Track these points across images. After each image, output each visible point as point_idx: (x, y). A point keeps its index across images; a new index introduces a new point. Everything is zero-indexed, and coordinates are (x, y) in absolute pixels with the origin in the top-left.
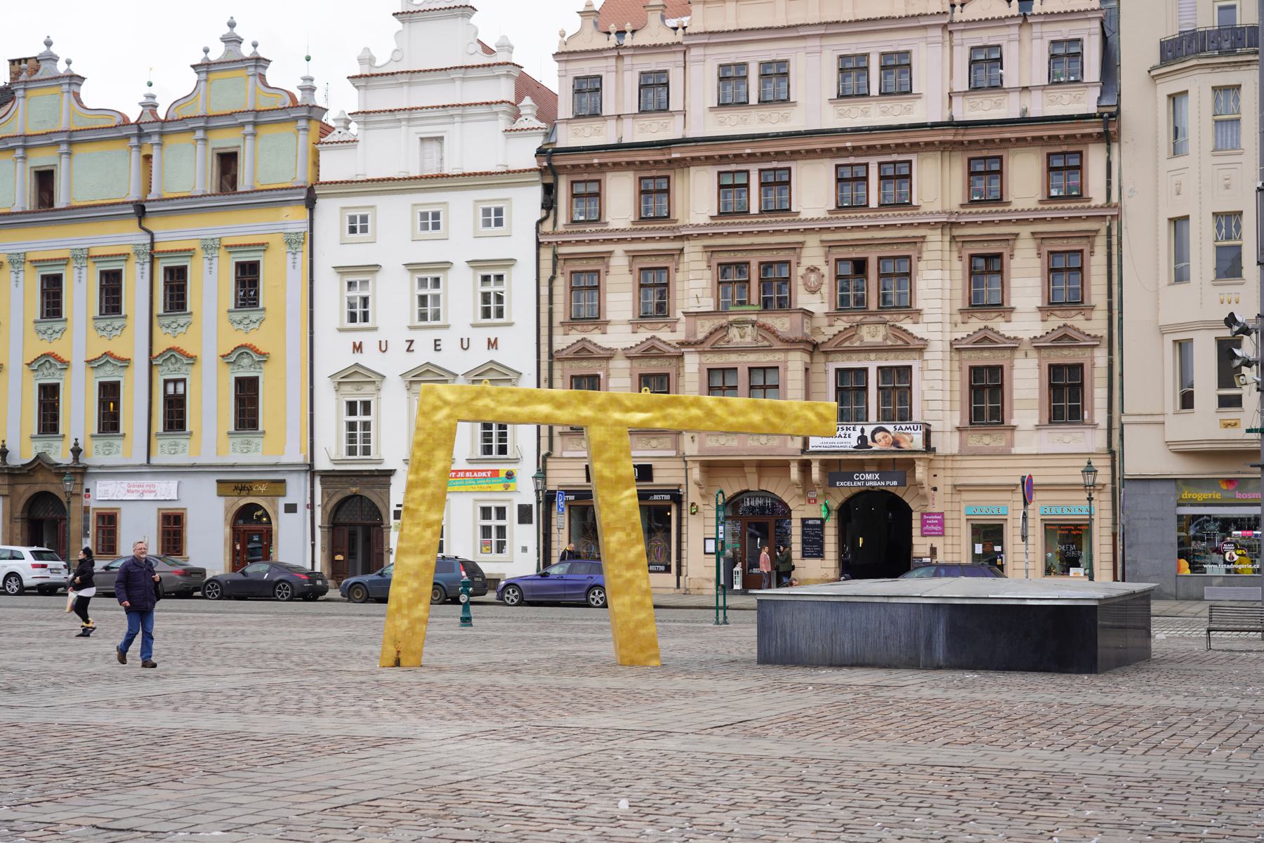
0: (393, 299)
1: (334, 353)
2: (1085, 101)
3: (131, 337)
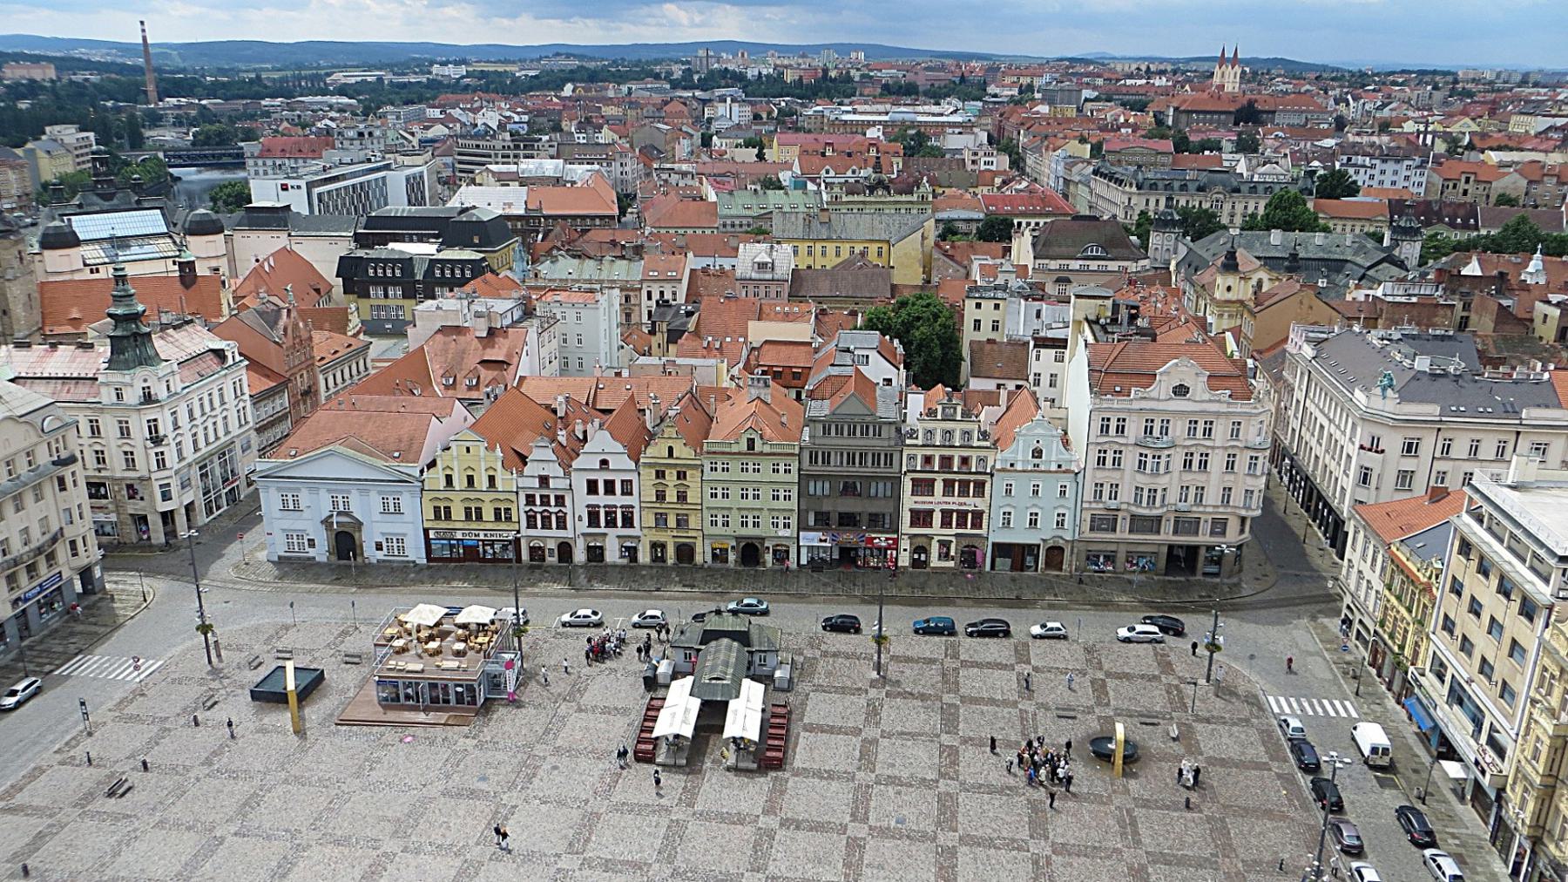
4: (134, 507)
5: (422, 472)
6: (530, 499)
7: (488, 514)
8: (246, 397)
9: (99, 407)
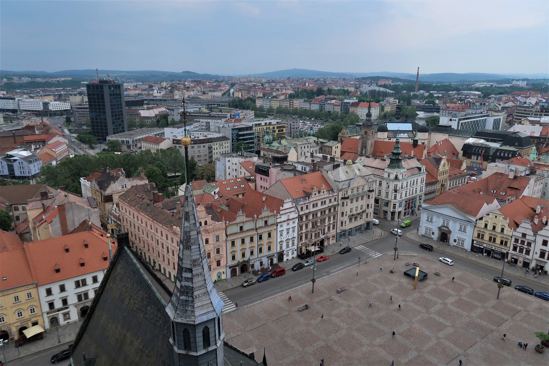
0: (285, 233)
1: (279, 240)
2: (336, 203)
3: (255, 243)
4: (385, 208)
5: (477, 220)
6: (516, 240)
7: (498, 241)
8: (424, 183)
9: (383, 178)
